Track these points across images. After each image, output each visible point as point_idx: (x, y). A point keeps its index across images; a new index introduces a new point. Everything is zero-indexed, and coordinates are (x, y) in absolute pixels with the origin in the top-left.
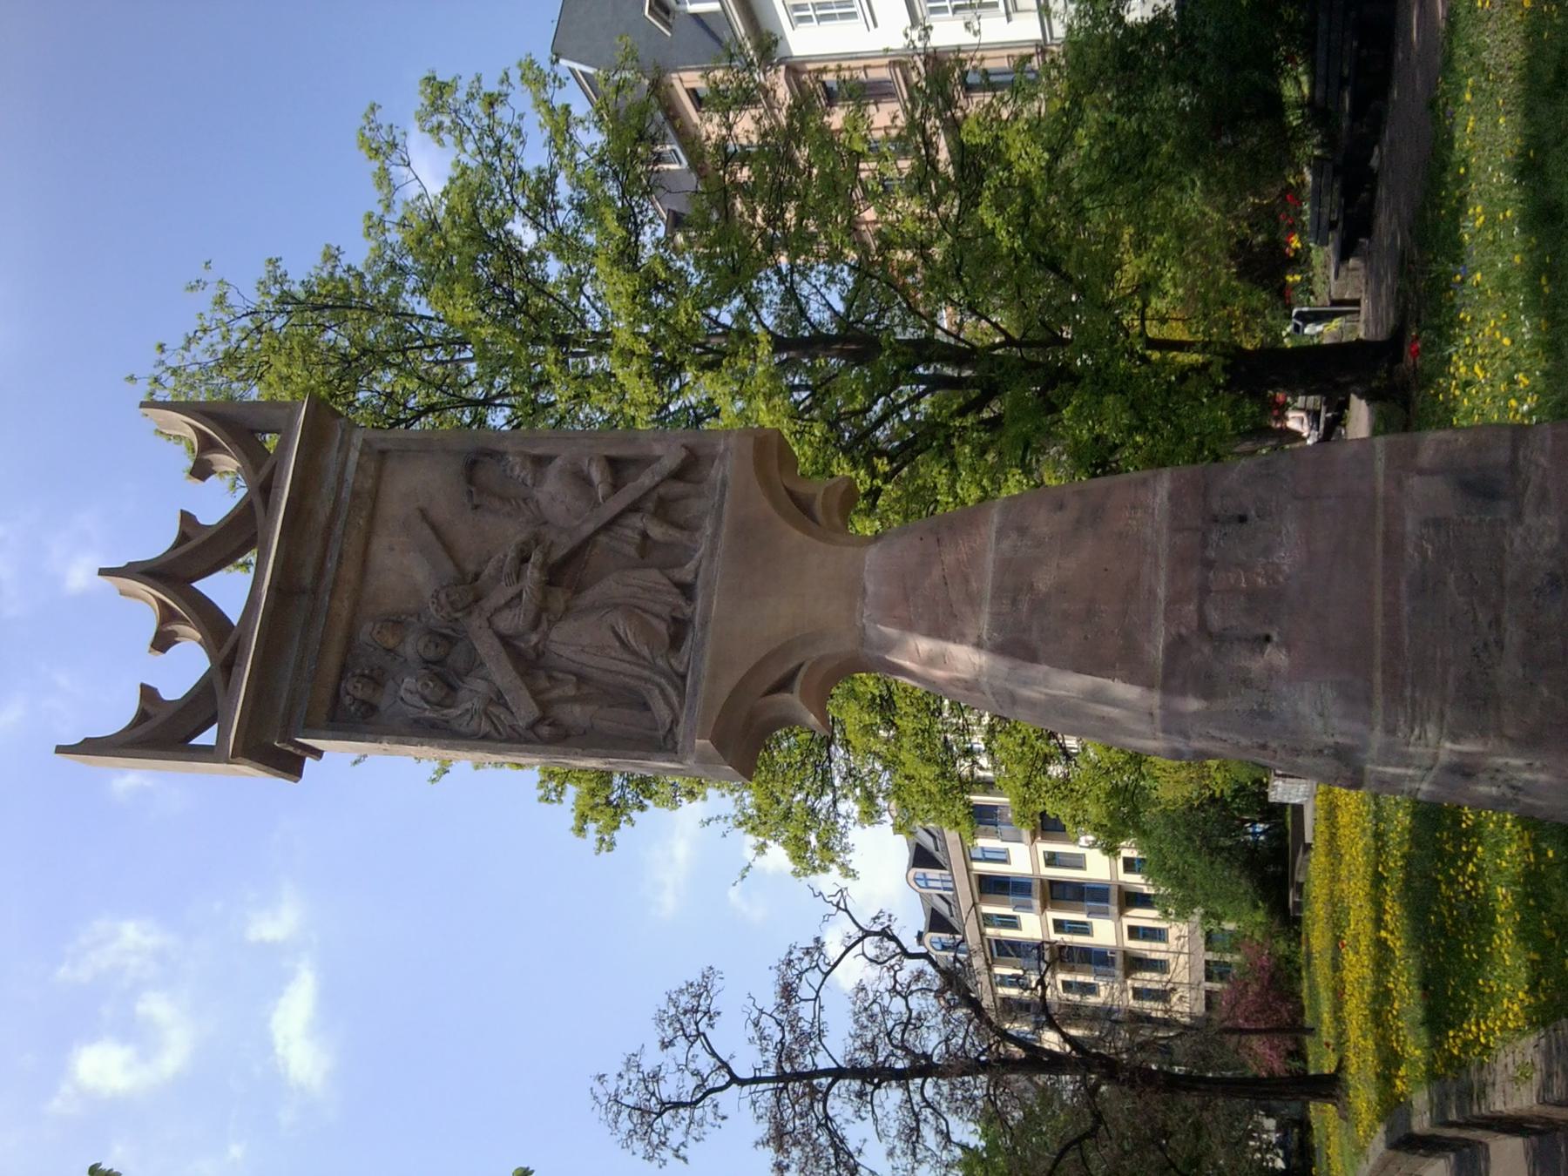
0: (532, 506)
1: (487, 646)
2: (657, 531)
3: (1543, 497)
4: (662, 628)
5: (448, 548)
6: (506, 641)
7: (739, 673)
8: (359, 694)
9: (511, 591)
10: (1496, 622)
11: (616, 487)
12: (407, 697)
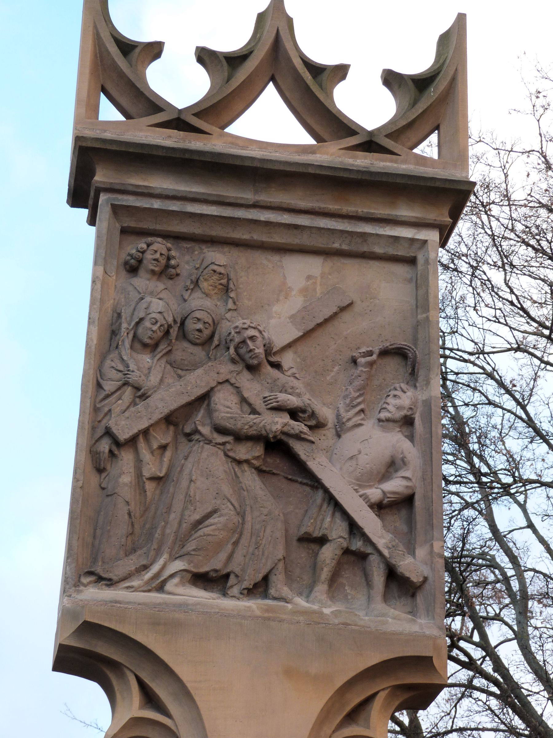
0: (357, 420)
1: (196, 382)
2: (328, 554)
6: (204, 398)
8: (149, 256)
9: (258, 404)
11: (379, 507)
12: (143, 304)
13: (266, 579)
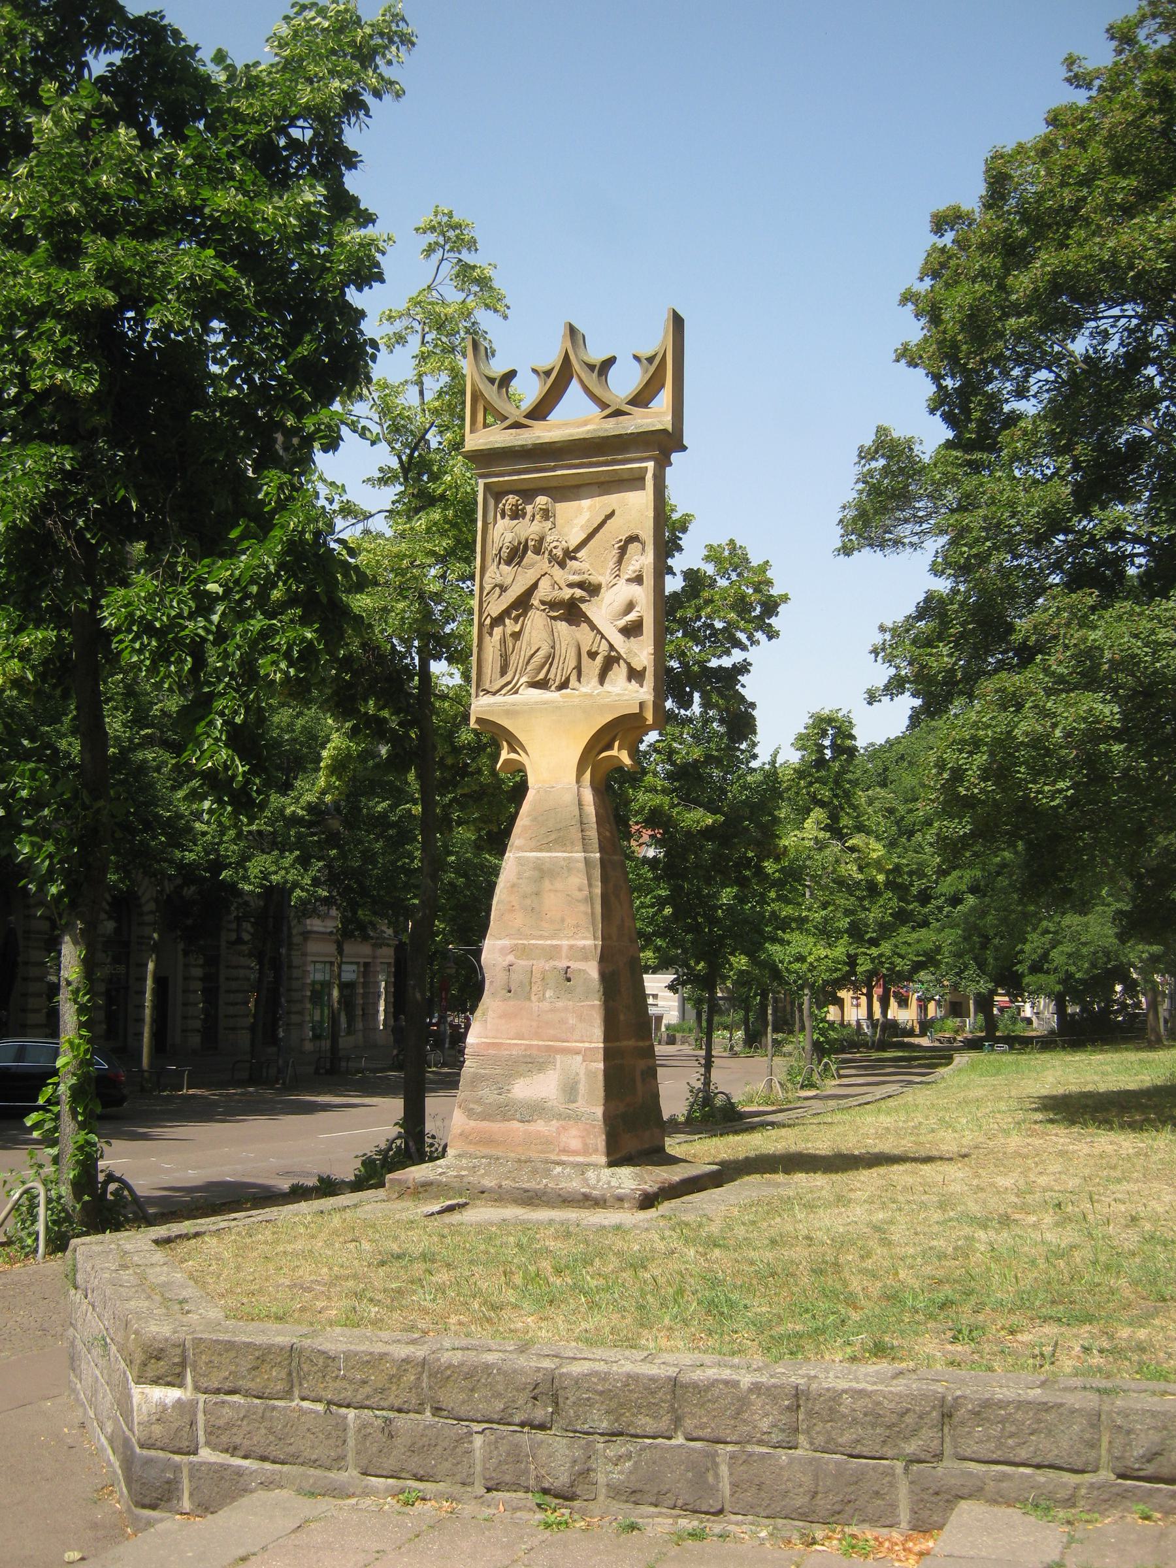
2: (599, 659)
4: (541, 676)
6: (535, 586)
9: (563, 585)
13: (568, 680)
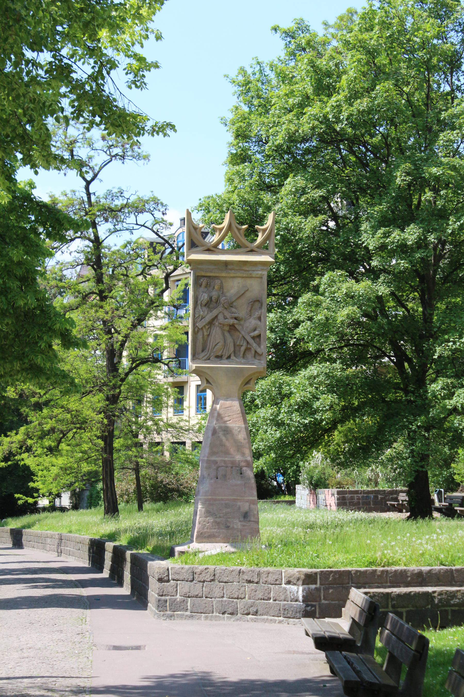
1: (215, 312)
2: (243, 349)
3: (244, 526)
4: (219, 354)
5: (239, 298)
6: (216, 317)
7: (209, 373)
9: (228, 316)
10: (220, 517)
